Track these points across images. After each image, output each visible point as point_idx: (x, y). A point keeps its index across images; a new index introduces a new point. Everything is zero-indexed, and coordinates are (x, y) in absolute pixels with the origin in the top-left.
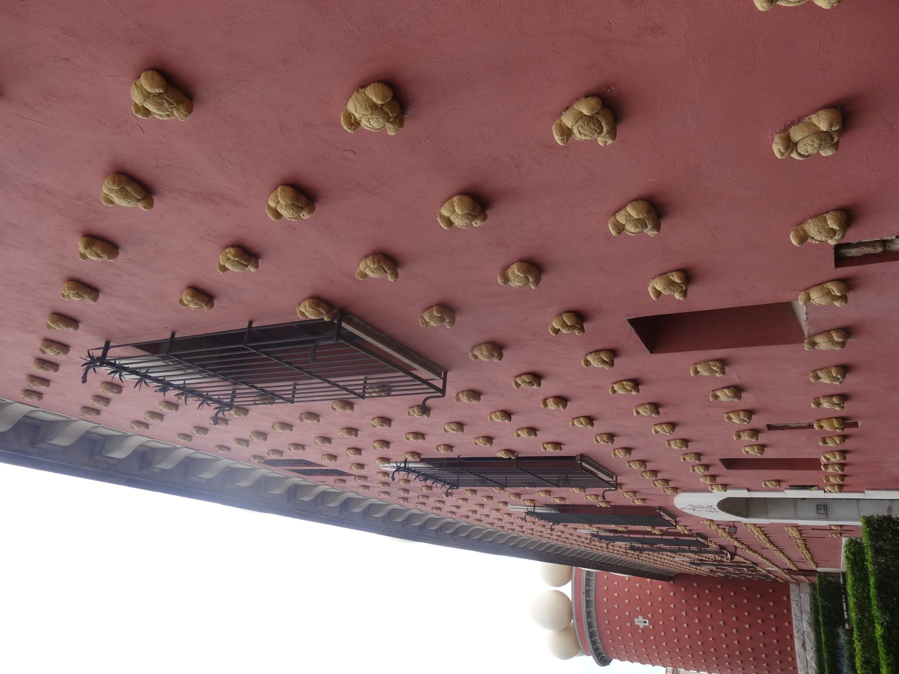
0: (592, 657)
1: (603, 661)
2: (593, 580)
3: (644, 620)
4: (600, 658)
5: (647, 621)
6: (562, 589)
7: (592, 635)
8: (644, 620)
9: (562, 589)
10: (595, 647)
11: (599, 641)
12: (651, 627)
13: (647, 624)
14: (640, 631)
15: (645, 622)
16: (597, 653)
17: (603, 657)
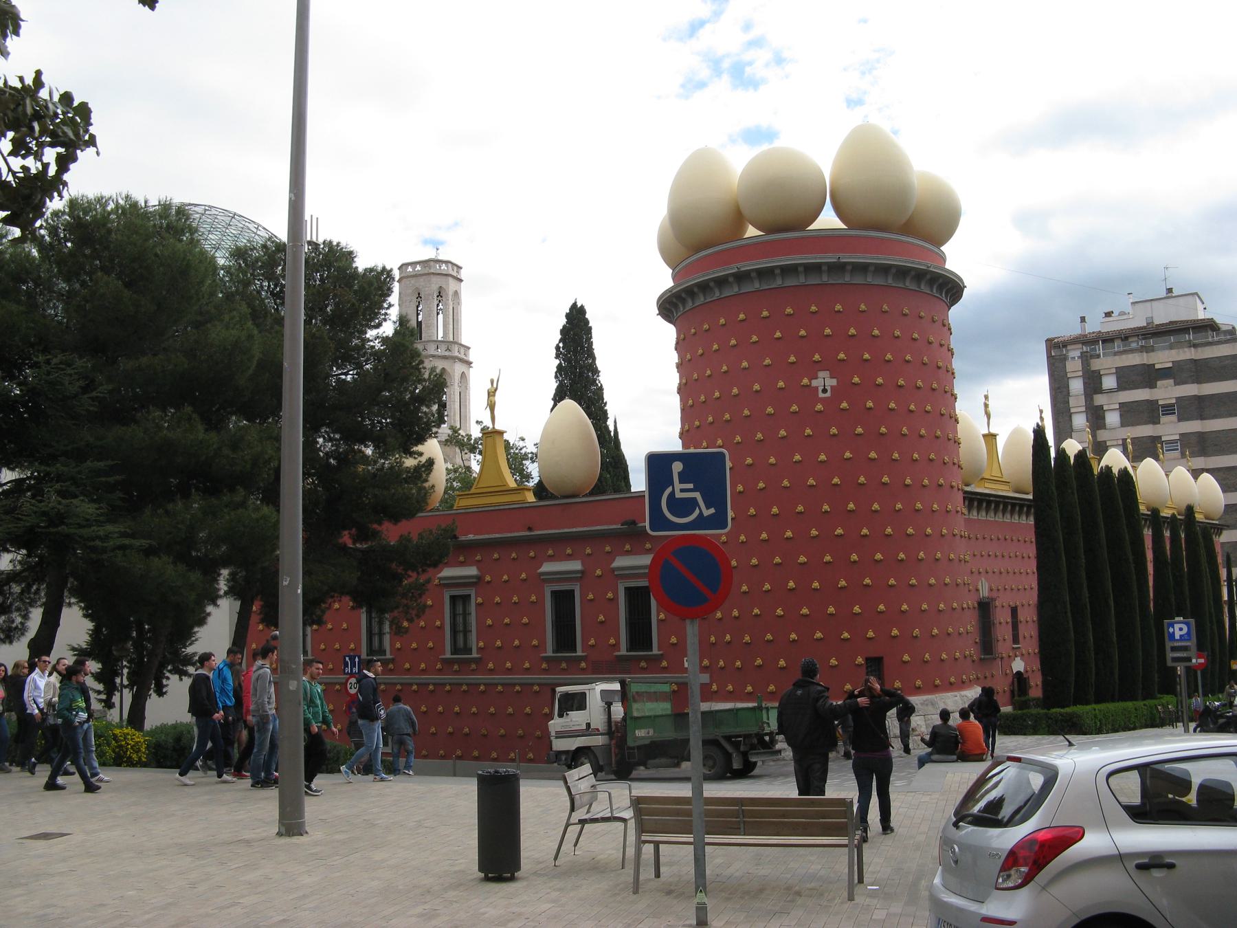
0: (673, 284)
1: (669, 306)
2: (905, 284)
3: (828, 388)
4: (683, 295)
5: (828, 394)
6: (828, 207)
7: (721, 282)
9: (828, 207)
10: (696, 290)
11: (727, 293)
12: (819, 407)
13: (821, 395)
14: (805, 381)
15: (825, 391)
16: (683, 295)
17: (683, 301)
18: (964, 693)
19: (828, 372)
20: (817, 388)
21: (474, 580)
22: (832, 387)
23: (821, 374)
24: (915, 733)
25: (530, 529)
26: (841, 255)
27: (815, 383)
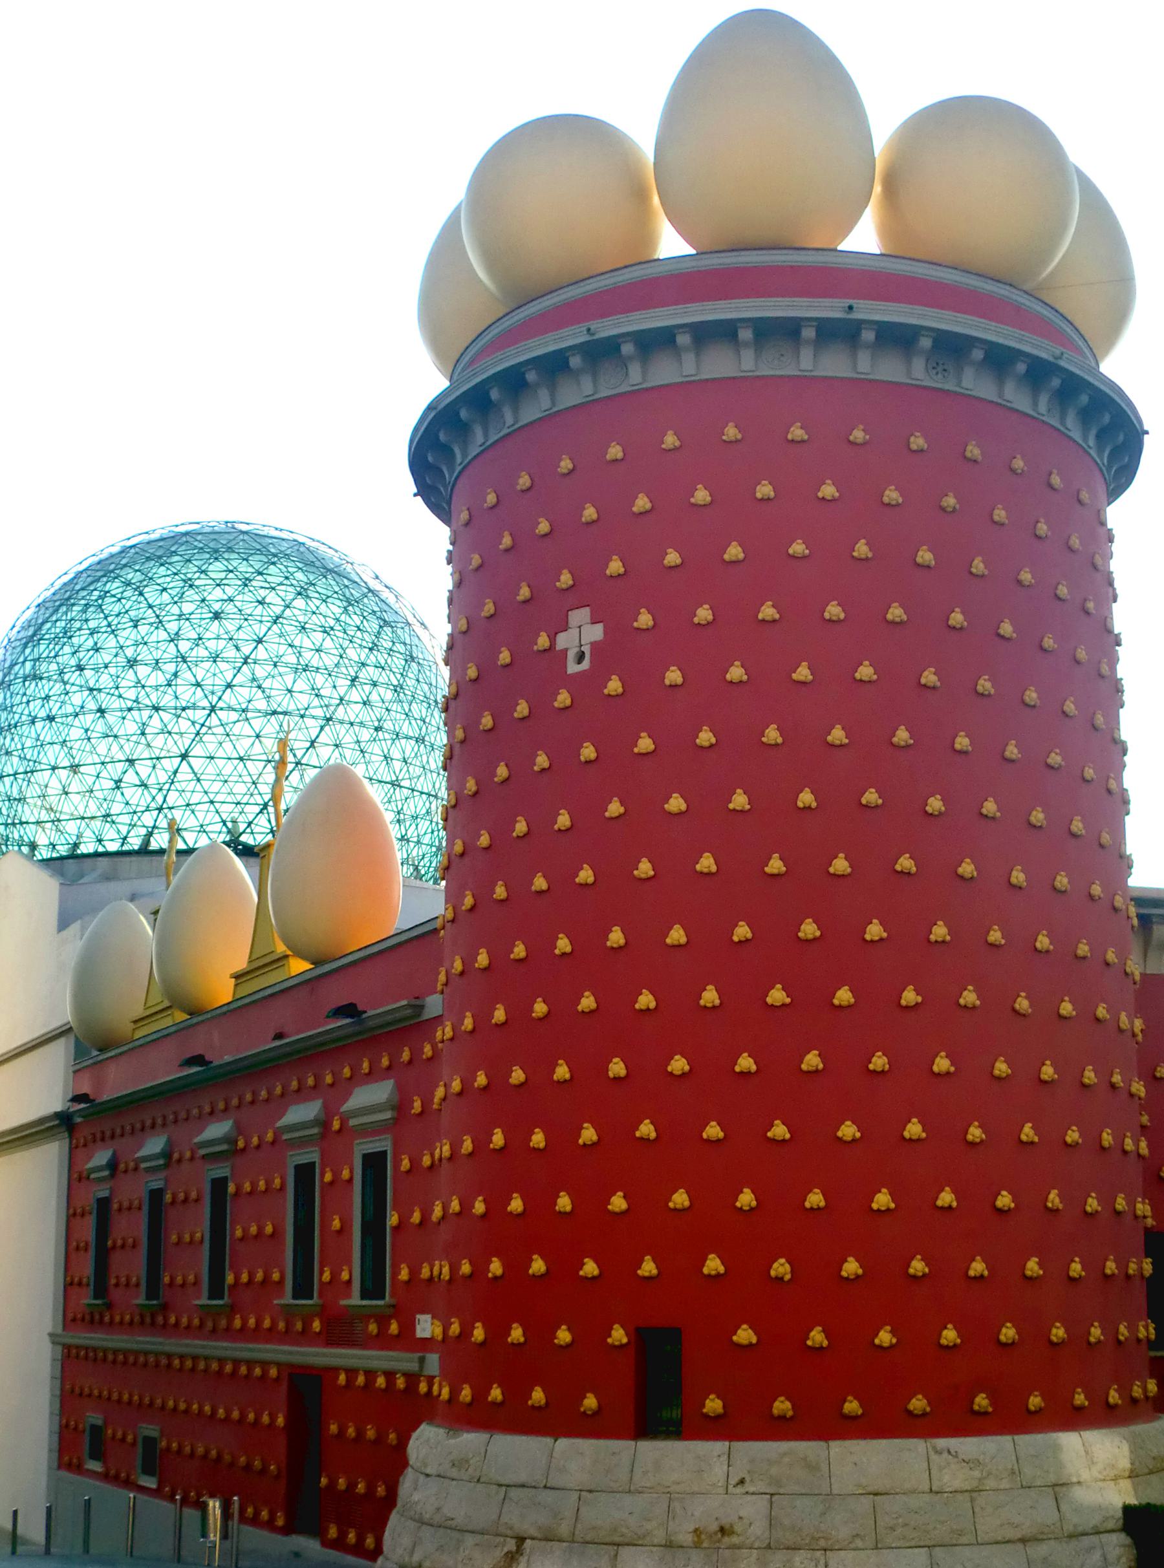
3: (587, 649)
5: (586, 664)
8: (587, 649)
12: (563, 698)
13: (572, 668)
14: (543, 641)
15: (581, 657)
18: (942, 1443)
19: (586, 611)
20: (565, 651)
21: (224, 1147)
22: (594, 645)
23: (579, 616)
24: (726, 1539)
25: (279, 1036)
26: (594, 325)
27: (562, 641)
